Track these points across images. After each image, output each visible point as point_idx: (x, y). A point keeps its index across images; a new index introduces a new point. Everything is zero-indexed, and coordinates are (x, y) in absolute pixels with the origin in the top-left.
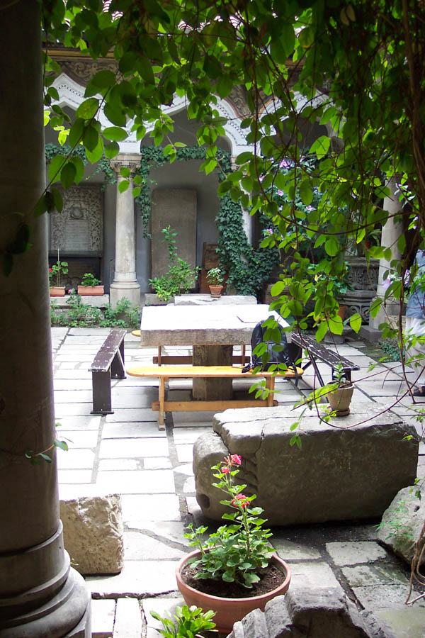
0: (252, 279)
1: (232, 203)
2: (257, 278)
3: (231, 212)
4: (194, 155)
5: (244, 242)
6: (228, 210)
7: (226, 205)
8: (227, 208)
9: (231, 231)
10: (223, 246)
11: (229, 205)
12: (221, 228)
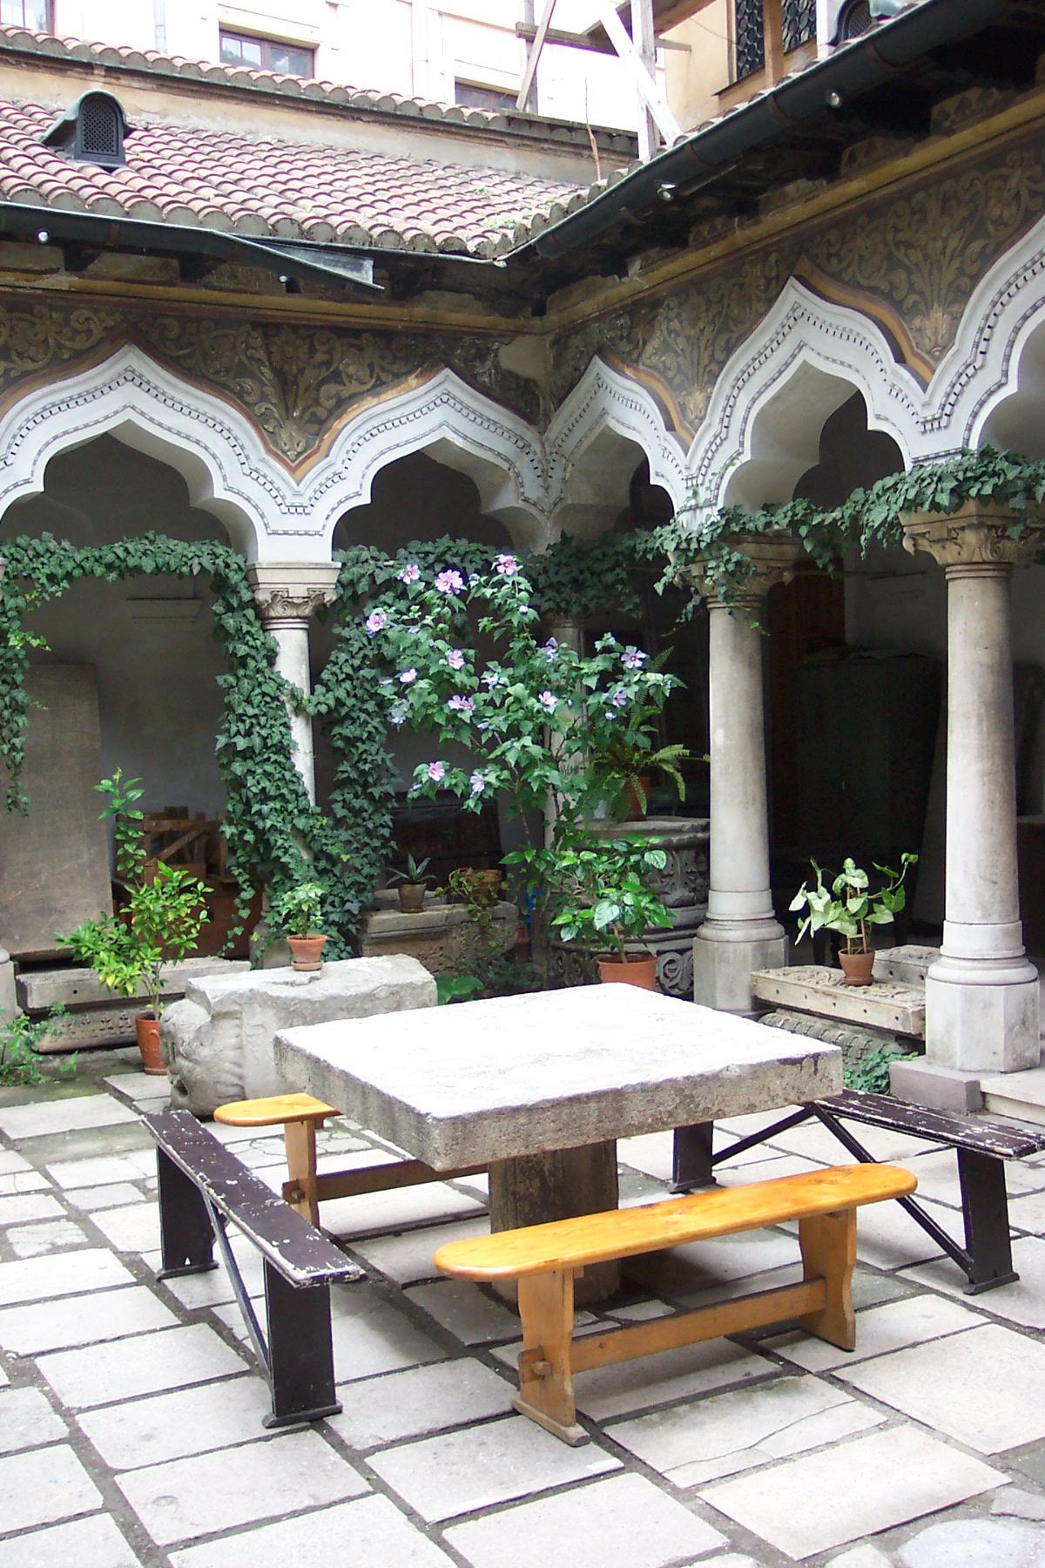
0: (332, 904)
1: (264, 694)
2: (343, 902)
3: (263, 720)
4: (148, 565)
5: (302, 804)
6: (255, 716)
7: (248, 701)
8: (251, 711)
9: (267, 774)
10: (246, 818)
11: (257, 700)
12: (238, 768)
